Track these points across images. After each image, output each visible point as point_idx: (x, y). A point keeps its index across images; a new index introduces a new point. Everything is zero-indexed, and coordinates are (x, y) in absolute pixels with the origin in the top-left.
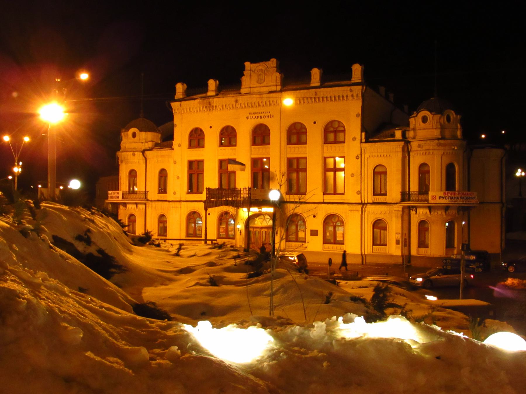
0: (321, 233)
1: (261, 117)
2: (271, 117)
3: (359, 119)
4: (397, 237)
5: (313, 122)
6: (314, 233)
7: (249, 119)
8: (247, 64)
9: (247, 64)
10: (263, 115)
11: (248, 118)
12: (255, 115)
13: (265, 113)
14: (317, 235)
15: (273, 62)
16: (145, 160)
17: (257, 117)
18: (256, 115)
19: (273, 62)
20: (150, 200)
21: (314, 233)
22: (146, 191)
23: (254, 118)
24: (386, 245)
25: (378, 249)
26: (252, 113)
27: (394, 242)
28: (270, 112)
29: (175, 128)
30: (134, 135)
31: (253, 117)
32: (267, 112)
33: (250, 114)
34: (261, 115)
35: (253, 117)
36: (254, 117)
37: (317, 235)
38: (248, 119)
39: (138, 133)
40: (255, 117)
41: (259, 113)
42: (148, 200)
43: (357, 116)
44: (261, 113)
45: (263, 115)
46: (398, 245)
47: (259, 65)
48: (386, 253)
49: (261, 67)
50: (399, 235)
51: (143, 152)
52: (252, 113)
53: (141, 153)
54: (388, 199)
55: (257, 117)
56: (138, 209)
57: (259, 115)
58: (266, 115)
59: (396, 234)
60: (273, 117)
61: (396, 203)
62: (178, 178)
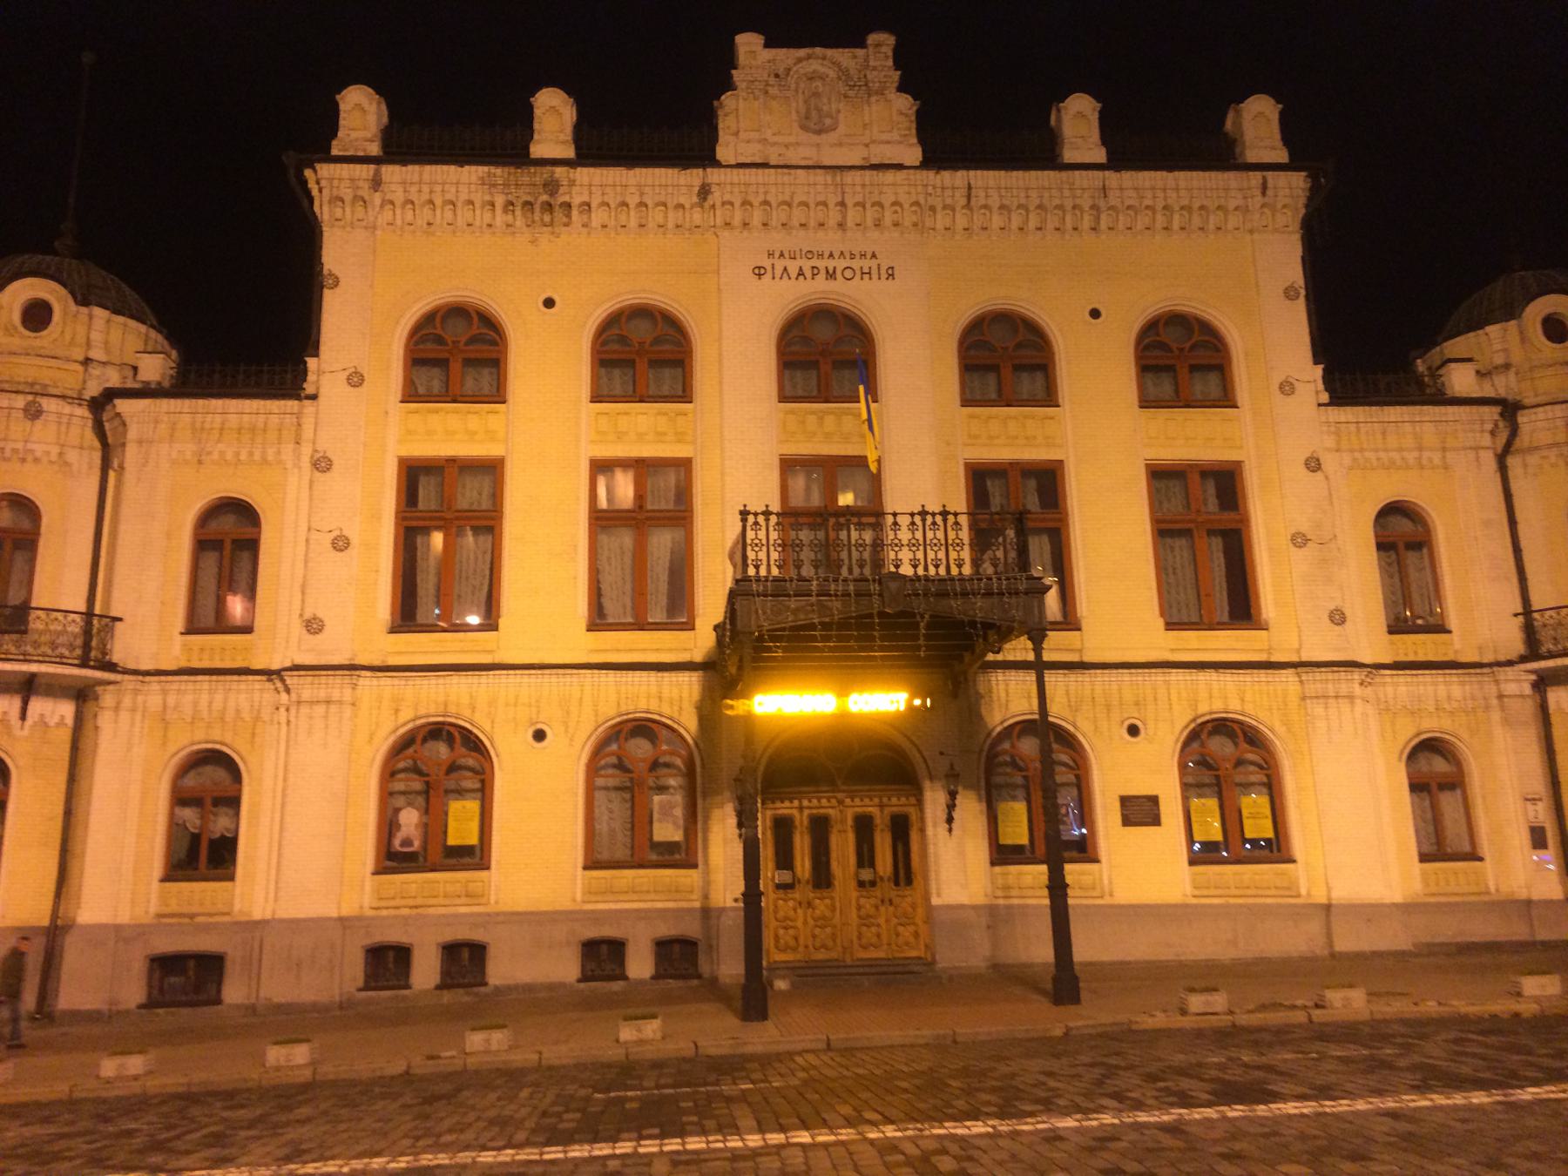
0: (1171, 809)
1: (831, 275)
2: (884, 276)
3: (1299, 310)
4: (1531, 814)
5: (1096, 306)
6: (1141, 811)
7: (767, 278)
8: (748, 44)
9: (748, 44)
10: (841, 264)
11: (759, 272)
12: (799, 262)
13: (852, 256)
14: (1155, 821)
15: (882, 43)
16: (97, 457)
17: (808, 273)
18: (807, 265)
19: (882, 43)
20: (131, 666)
21: (1141, 811)
22: (89, 615)
23: (794, 275)
24: (1474, 856)
25: (1453, 877)
26: (782, 255)
27: (1519, 838)
28: (874, 256)
29: (326, 292)
30: (37, 316)
31: (785, 269)
32: (863, 255)
33: (771, 255)
34: (831, 264)
35: (785, 269)
36: (793, 272)
37: (1155, 821)
38: (760, 275)
39: (65, 313)
40: (801, 273)
41: (821, 256)
42: (111, 667)
43: (1290, 294)
44: (831, 255)
45: (841, 264)
46: (1542, 853)
47: (809, 57)
48: (1488, 893)
49: (814, 65)
50: (1539, 803)
51: (101, 404)
52: (782, 255)
53: (83, 412)
54: (1458, 645)
55: (808, 273)
56: (29, 721)
57: (821, 264)
58: (856, 264)
59: (1527, 800)
60: (891, 276)
61: (1510, 663)
62: (341, 544)
